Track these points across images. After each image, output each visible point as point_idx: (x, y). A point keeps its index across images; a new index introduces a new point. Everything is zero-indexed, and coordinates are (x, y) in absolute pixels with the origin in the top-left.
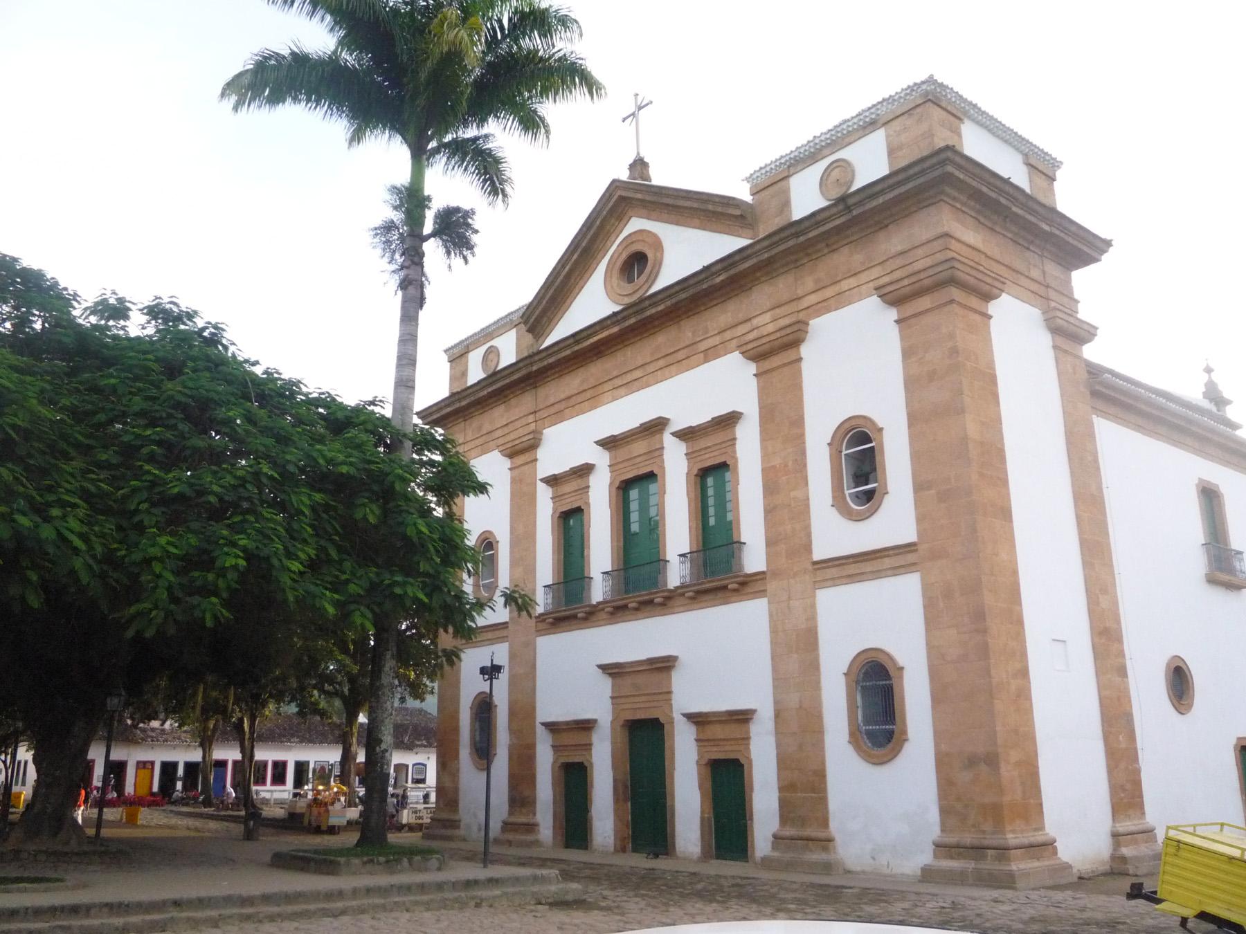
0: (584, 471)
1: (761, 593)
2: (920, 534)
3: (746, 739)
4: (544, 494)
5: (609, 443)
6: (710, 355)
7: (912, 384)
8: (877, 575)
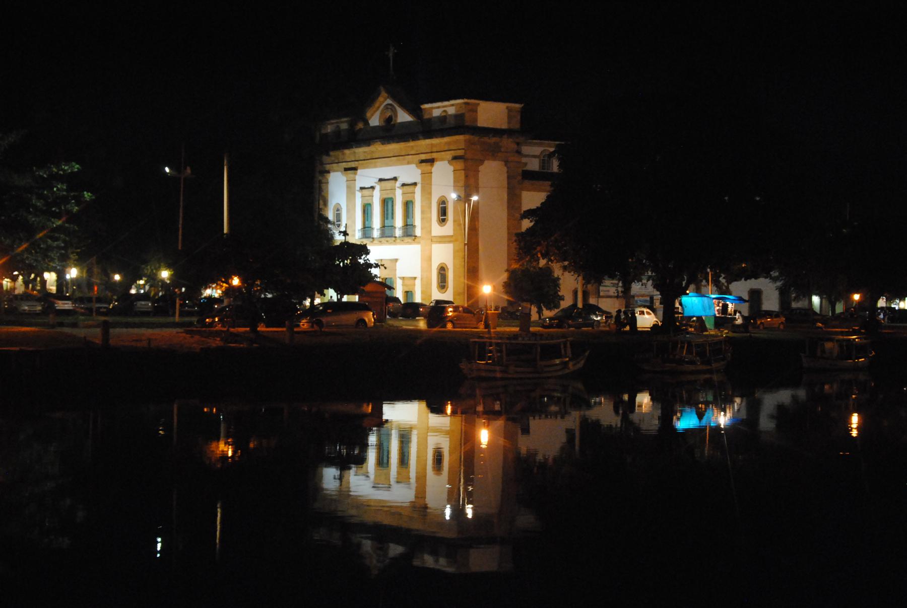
1: (419, 243)
2: (454, 233)
3: (414, 285)
4: (358, 195)
8: (444, 242)
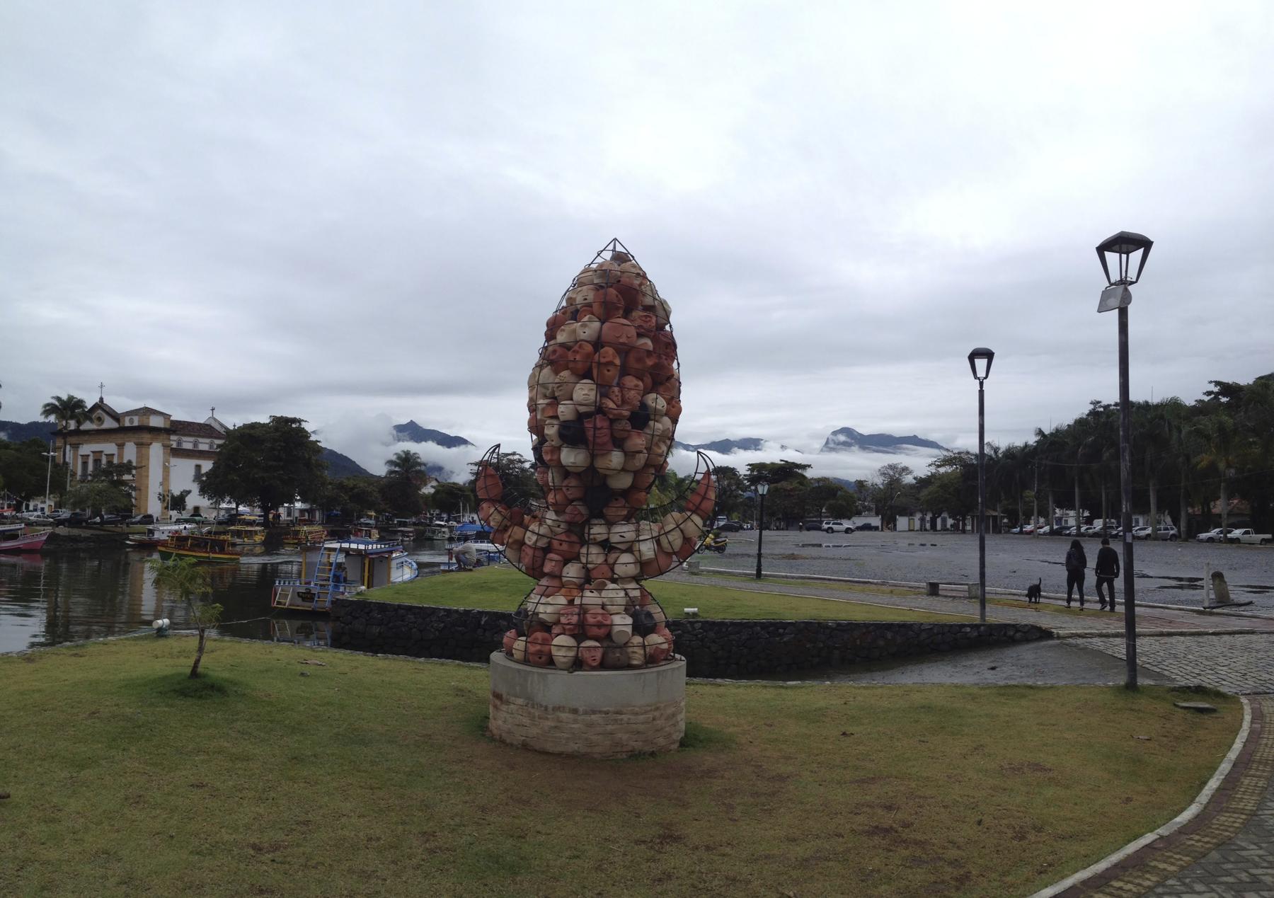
0: (88, 455)
5: (93, 452)
6: (111, 442)
7: (137, 457)
